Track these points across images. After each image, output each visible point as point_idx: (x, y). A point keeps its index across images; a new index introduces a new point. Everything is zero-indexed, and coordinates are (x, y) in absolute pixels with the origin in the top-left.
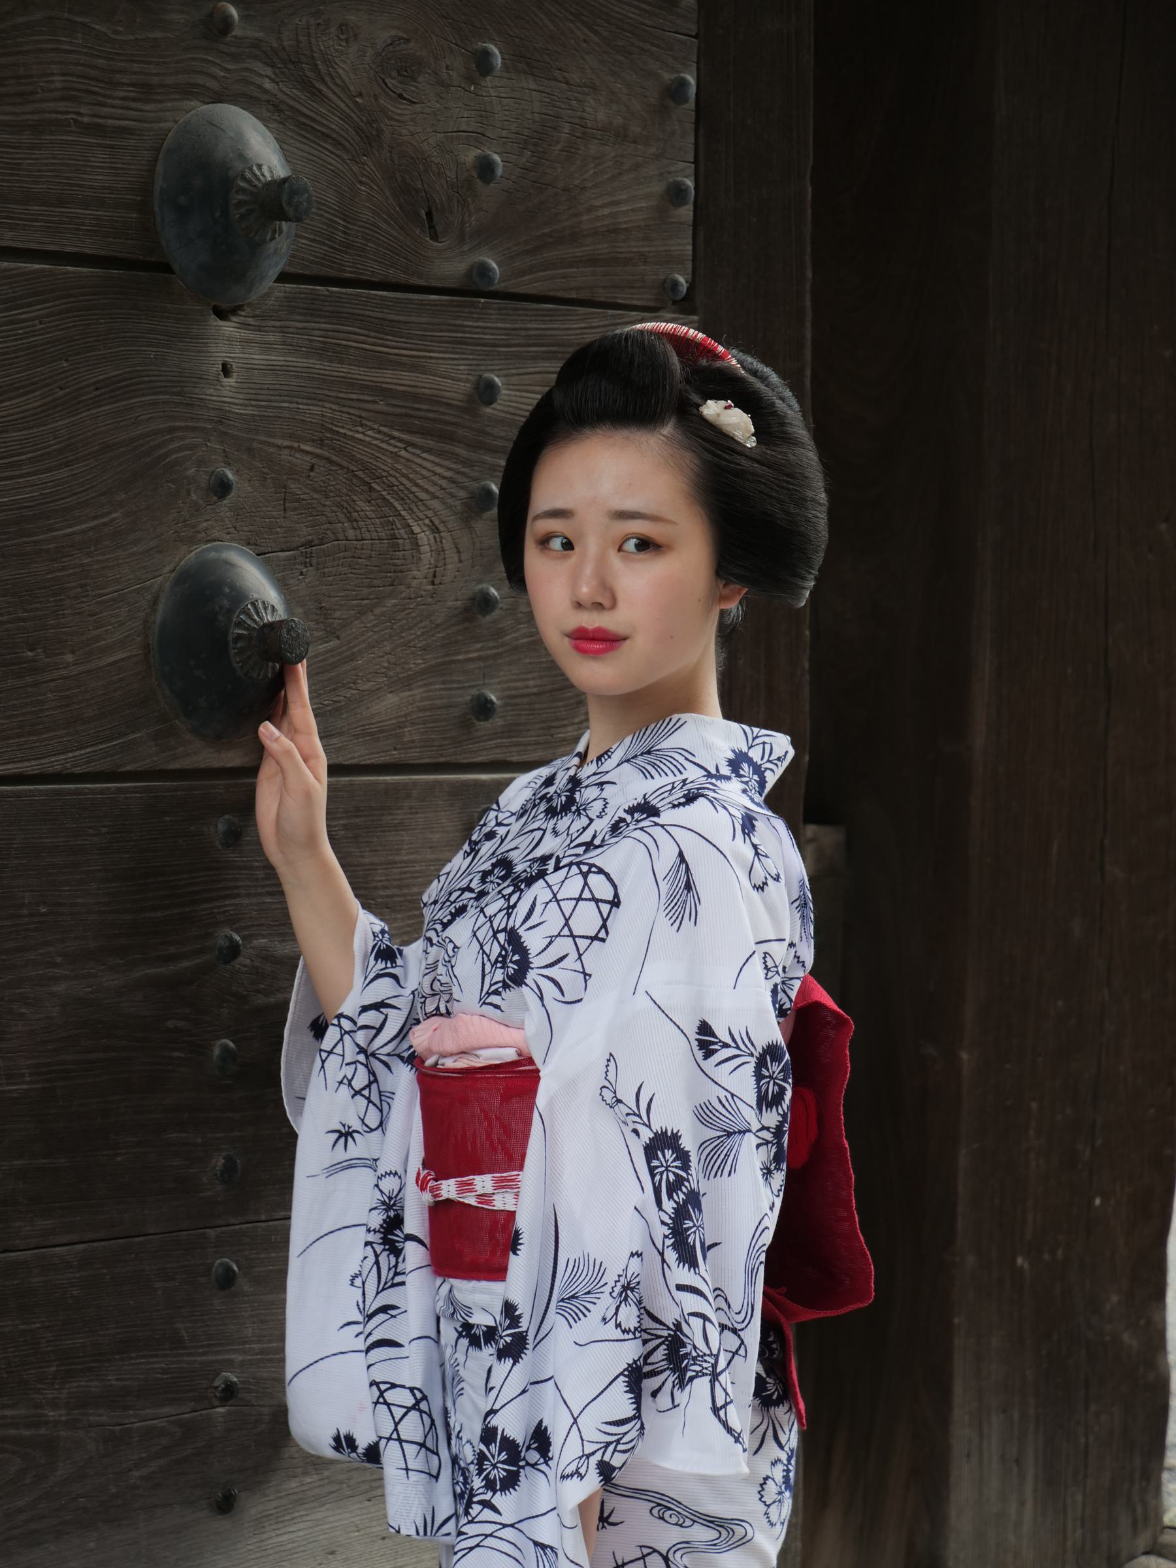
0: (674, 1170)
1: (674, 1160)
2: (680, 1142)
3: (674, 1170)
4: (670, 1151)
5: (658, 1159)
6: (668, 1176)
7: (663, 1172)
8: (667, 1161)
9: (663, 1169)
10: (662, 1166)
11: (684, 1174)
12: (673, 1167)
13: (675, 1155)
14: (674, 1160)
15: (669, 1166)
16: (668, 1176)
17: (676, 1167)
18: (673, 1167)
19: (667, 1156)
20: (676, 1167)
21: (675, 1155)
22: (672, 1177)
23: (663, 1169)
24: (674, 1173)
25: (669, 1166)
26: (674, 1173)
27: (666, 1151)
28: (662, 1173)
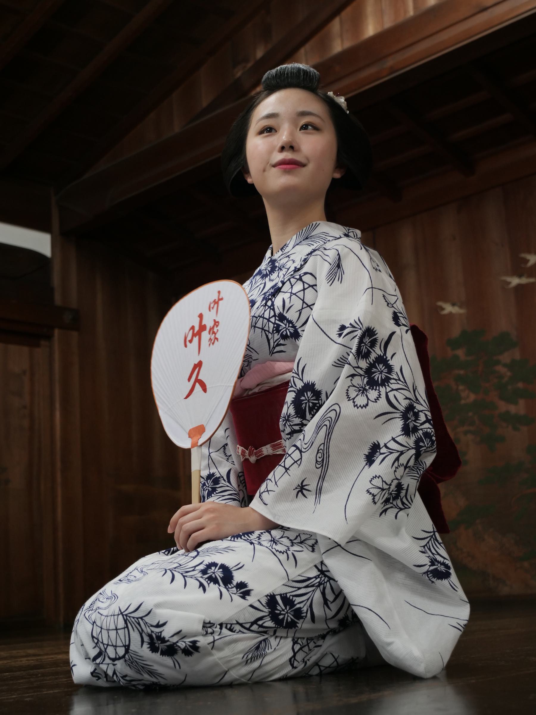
0: (312, 401)
1: (312, 397)
2: (315, 387)
3: (312, 401)
4: (310, 392)
5: (304, 396)
6: (309, 404)
7: (307, 402)
8: (308, 398)
9: (307, 401)
10: (306, 400)
11: (317, 402)
12: (311, 400)
13: (312, 394)
14: (312, 397)
15: (310, 400)
16: (309, 404)
17: (313, 400)
18: (311, 400)
19: (309, 395)
20: (313, 400)
21: (312, 394)
22: (311, 404)
23: (307, 401)
24: (312, 403)
25: (310, 400)
26: (312, 403)
27: (308, 392)
28: (306, 403)
